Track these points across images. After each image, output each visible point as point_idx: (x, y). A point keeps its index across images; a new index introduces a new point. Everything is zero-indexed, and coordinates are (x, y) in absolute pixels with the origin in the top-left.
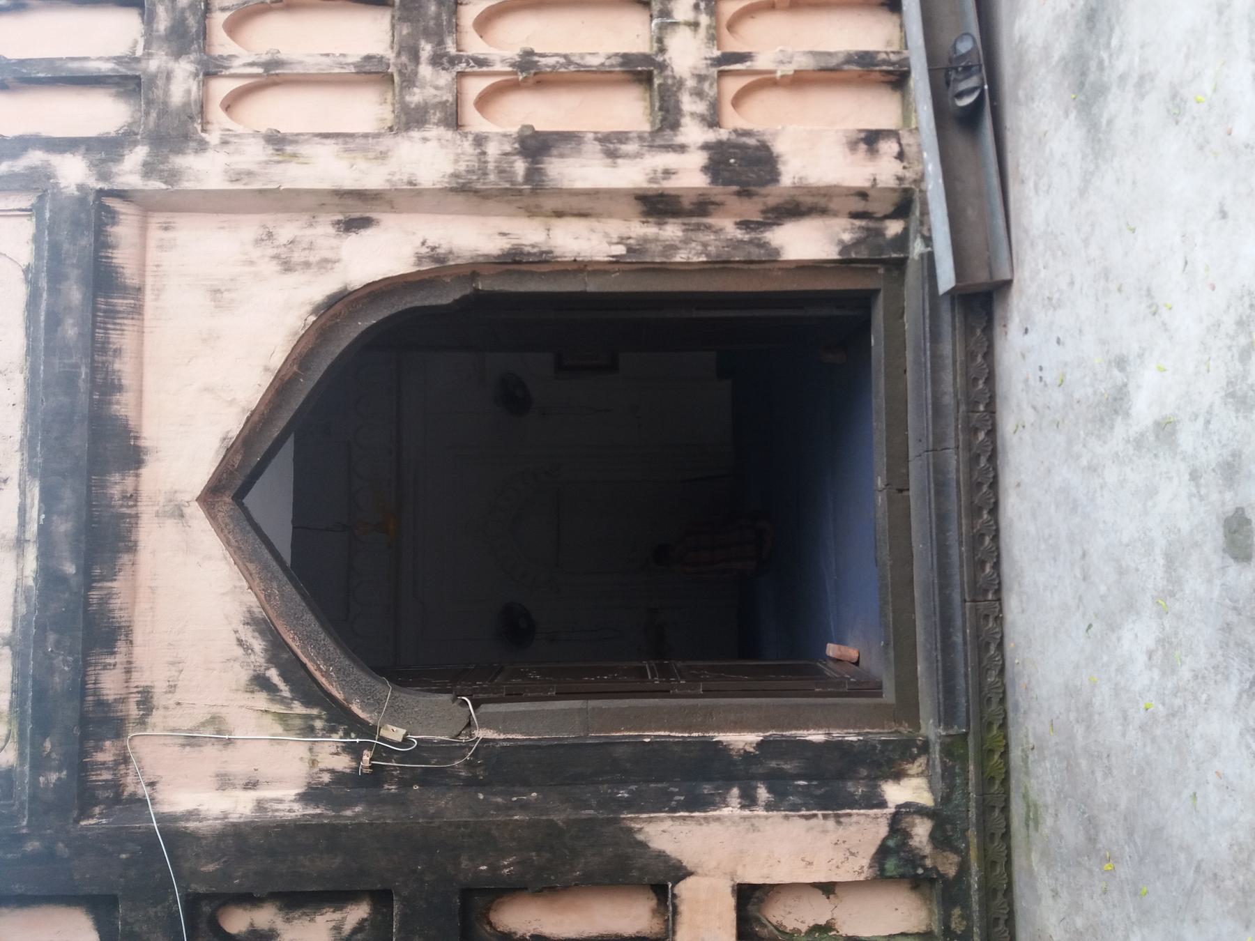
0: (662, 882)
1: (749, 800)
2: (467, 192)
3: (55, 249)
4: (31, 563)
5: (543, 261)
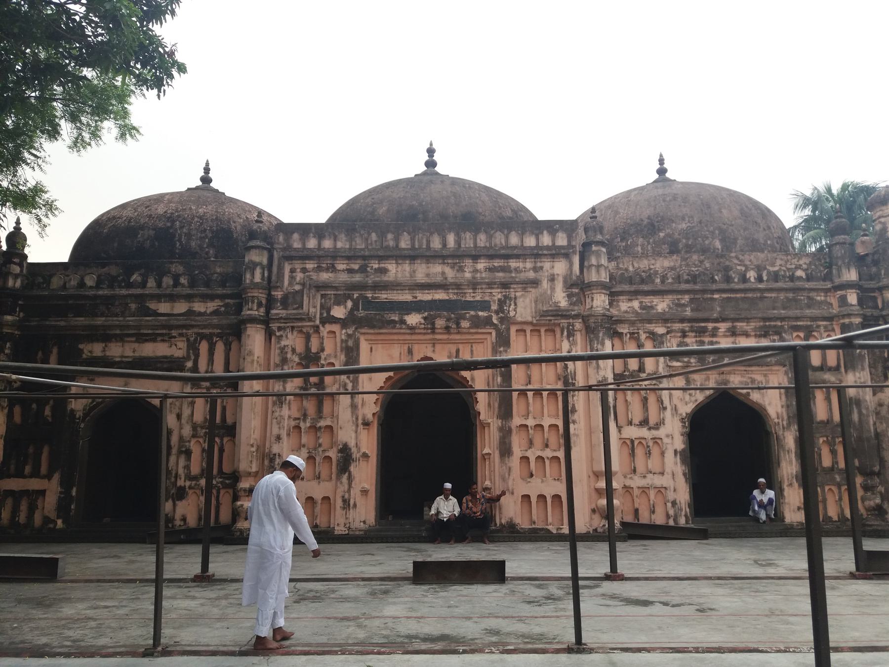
0: (49, 477)
1: (61, 493)
2: (181, 438)
3: (174, 362)
4: (117, 359)
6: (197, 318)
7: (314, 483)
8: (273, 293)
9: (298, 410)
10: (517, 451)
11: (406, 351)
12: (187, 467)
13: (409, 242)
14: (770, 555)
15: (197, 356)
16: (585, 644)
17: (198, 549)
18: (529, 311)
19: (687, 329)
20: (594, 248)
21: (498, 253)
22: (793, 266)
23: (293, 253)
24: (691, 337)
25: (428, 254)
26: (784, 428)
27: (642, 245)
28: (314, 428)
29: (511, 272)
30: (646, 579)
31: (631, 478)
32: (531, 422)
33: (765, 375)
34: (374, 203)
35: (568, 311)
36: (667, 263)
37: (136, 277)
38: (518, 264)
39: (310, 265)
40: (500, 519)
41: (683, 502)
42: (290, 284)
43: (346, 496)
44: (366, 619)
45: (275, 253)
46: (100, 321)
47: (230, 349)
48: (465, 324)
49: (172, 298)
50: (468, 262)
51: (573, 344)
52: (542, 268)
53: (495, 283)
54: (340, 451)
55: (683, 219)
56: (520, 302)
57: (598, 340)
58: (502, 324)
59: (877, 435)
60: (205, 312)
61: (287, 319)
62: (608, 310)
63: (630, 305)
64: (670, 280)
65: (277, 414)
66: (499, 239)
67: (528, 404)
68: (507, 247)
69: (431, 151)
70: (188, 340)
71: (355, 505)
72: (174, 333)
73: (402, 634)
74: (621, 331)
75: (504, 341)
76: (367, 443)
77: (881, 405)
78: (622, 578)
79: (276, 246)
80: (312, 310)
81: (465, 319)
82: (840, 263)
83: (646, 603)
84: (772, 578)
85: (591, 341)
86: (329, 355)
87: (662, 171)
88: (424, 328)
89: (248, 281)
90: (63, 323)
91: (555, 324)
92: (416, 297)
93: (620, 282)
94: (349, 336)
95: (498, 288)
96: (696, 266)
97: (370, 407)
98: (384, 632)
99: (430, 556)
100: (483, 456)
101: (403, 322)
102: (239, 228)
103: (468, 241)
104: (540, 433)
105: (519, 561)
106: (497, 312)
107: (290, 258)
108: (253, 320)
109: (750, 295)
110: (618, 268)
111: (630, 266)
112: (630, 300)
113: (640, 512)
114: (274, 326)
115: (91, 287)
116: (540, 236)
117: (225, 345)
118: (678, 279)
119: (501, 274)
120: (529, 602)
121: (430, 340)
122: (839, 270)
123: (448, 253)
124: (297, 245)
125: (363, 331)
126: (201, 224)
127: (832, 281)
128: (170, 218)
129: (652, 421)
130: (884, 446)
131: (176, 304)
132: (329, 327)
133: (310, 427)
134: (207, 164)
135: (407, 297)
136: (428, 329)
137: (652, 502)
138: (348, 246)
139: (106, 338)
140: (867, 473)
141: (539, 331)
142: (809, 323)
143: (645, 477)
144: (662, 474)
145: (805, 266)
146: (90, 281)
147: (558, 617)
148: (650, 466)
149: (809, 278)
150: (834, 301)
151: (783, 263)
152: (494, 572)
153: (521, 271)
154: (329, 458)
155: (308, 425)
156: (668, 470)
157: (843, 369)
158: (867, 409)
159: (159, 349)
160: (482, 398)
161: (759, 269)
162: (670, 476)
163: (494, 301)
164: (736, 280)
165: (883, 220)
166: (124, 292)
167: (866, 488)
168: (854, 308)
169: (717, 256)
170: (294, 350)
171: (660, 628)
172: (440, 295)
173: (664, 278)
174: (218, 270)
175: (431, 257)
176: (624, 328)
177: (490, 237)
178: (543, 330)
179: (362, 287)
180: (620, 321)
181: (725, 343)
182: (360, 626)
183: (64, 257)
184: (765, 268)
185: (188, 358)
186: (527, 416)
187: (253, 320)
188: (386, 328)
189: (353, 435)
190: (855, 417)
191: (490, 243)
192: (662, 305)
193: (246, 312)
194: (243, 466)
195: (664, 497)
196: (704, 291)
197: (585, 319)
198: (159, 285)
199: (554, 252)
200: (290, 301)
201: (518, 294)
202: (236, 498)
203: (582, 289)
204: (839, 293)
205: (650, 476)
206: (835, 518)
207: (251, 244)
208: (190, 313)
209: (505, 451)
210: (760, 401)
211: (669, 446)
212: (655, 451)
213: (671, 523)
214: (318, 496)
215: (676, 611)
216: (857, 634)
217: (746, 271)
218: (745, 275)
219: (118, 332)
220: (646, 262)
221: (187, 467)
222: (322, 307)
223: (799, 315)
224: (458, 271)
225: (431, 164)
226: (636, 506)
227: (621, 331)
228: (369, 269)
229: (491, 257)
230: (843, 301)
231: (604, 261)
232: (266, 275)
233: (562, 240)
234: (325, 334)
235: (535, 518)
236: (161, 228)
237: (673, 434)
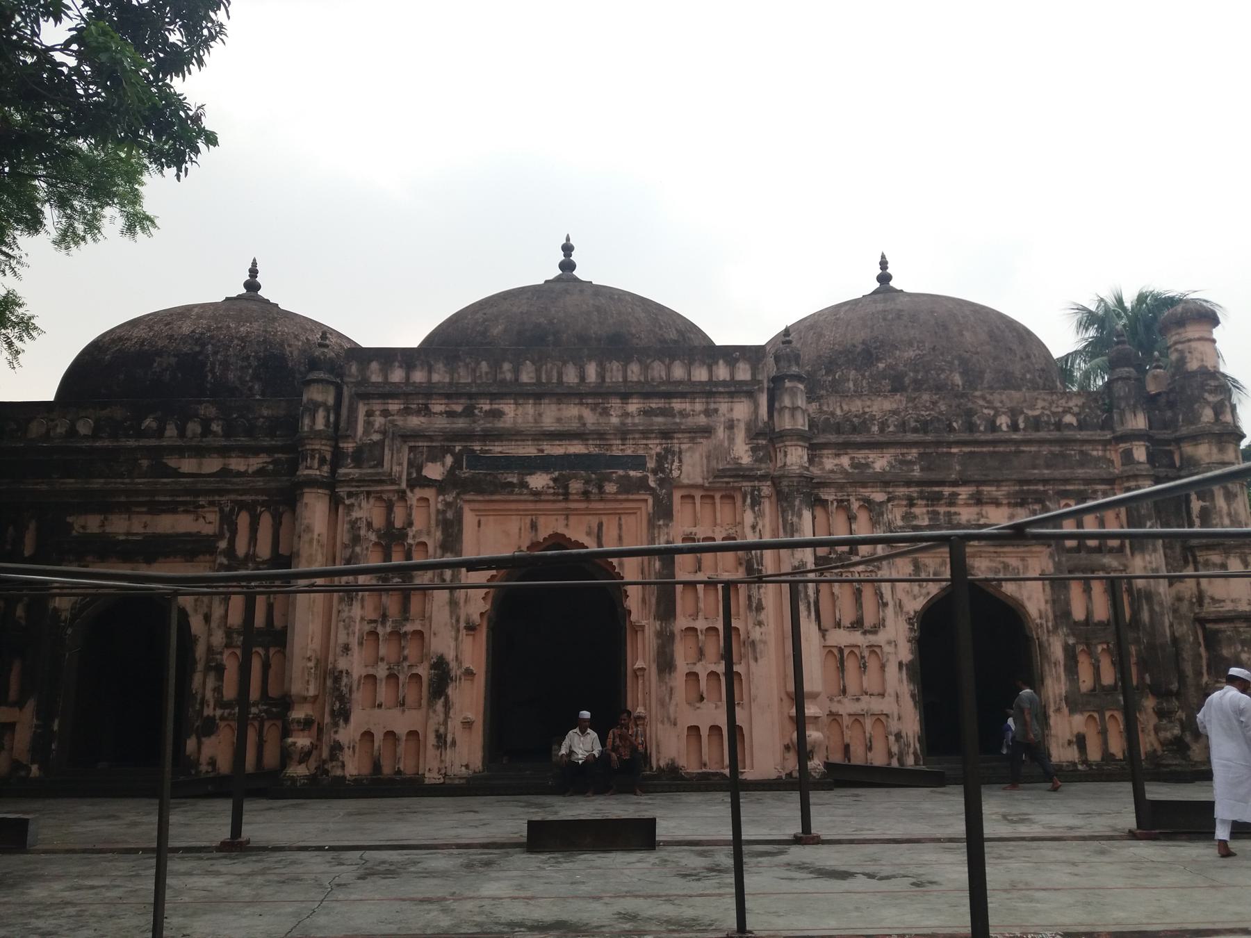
0: (20, 704)
1: (37, 727)
2: (210, 649)
4: (122, 538)
5: (194, 671)
6: (235, 480)
7: (396, 712)
8: (341, 445)
9: (375, 609)
10: (682, 664)
11: (528, 525)
12: (218, 690)
13: (533, 375)
14: (1025, 808)
15: (234, 532)
16: (750, 932)
17: (226, 805)
18: (698, 469)
19: (915, 495)
20: (788, 384)
21: (657, 389)
22: (1060, 410)
23: (371, 390)
24: (921, 506)
25: (559, 391)
26: (1048, 632)
27: (855, 381)
28: (397, 635)
29: (674, 416)
30: (851, 842)
31: (839, 702)
32: (701, 624)
33: (1023, 559)
34: (485, 320)
35: (752, 469)
36: (888, 405)
37: (149, 422)
38: (683, 406)
39: (394, 406)
40: (658, 760)
41: (911, 734)
42: (366, 432)
43: (442, 730)
44: (455, 900)
45: (345, 388)
46: (97, 483)
47: (281, 523)
48: (610, 488)
49: (200, 452)
50: (615, 403)
51: (759, 515)
52: (716, 411)
53: (652, 432)
54: (434, 666)
55: (911, 344)
56: (686, 458)
57: (792, 507)
58: (661, 488)
59: (1175, 640)
60: (246, 471)
61: (361, 481)
62: (807, 469)
63: (836, 461)
64: (891, 429)
65: (344, 615)
66: (658, 370)
67: (697, 599)
68: (669, 382)
69: (568, 249)
70: (221, 511)
71: (454, 743)
72: (202, 500)
73: (503, 921)
74: (826, 497)
75: (664, 512)
76: (472, 655)
77: (1179, 599)
78: (817, 841)
79: (347, 379)
80: (396, 468)
81: (610, 481)
82: (1123, 405)
83: (844, 875)
84: (1023, 839)
85: (784, 511)
86: (420, 532)
87: (884, 278)
88: (554, 494)
89: (306, 429)
90: (44, 487)
91: (734, 488)
92: (542, 451)
93: (824, 431)
94: (448, 505)
95: (656, 438)
96: (927, 409)
97: (476, 605)
98: (477, 919)
99: (556, 813)
100: (635, 671)
101: (524, 485)
102: (296, 353)
103: (615, 373)
104: (714, 638)
105: (680, 819)
106: (655, 472)
107: (365, 397)
108: (313, 483)
109: (1001, 449)
110: (821, 411)
111: (837, 408)
112: (838, 455)
113: (852, 748)
114: (342, 491)
115: (85, 436)
116: (714, 368)
117: (274, 517)
118: (903, 426)
119: (660, 419)
120: (685, 876)
121: (562, 510)
122: (1122, 414)
123: (588, 390)
124: (376, 378)
125: (467, 497)
126: (243, 348)
127: (1112, 429)
128: (199, 340)
129: (869, 621)
130: (1185, 655)
131: (204, 461)
132: (419, 493)
133: (391, 633)
134: (254, 264)
135: (529, 450)
136: (558, 494)
137: (868, 735)
138: (447, 380)
139: (105, 505)
140: (1160, 692)
141: (713, 497)
142: (1082, 487)
143: (858, 700)
144: (882, 695)
145: (1076, 410)
146: (84, 428)
147: (720, 895)
148: (865, 685)
149: (1082, 426)
150: (1115, 457)
151: (1046, 404)
152: (640, 836)
153: (688, 415)
154: (417, 677)
155: (389, 629)
156: (890, 690)
157: (1128, 551)
158: (1161, 604)
159: (183, 524)
160: (634, 593)
161: (1014, 413)
162: (893, 699)
163: (651, 457)
164: (982, 428)
165: (1179, 347)
166: (132, 443)
167: (1161, 713)
168: (1142, 467)
169: (956, 396)
170: (369, 525)
171: (857, 909)
172: (576, 448)
173: (883, 426)
174: (265, 413)
175: (563, 395)
176: (829, 494)
177: (645, 368)
178: (718, 496)
179: (468, 436)
180: (823, 485)
181: (966, 514)
182: (445, 911)
183: (50, 396)
184: (1022, 412)
185: (219, 536)
186: (695, 616)
187: (313, 483)
188: (500, 494)
189: (452, 644)
190: (1145, 616)
191: (646, 377)
192: (880, 462)
193: (303, 472)
194: (296, 688)
195: (885, 727)
196: (938, 444)
197: (775, 481)
198: (182, 433)
199: (733, 389)
200: (365, 456)
201: (683, 447)
202: (286, 733)
203: (771, 440)
204: (1123, 446)
205: (865, 698)
206: (1120, 756)
207: (312, 376)
208: (225, 472)
209: (666, 664)
210: (1017, 595)
211: (892, 658)
212: (873, 664)
213: (895, 763)
214: (402, 731)
215: (884, 886)
216: (1122, 915)
217: (997, 414)
218: (994, 422)
219: (123, 499)
220: (859, 403)
221: (218, 690)
222: (410, 464)
223: (1068, 476)
224: (601, 414)
225: (567, 266)
226: (847, 740)
227: (824, 497)
228: (476, 411)
229: (646, 396)
230: (1128, 456)
231: (801, 402)
232: (332, 419)
233: (743, 373)
234: (414, 502)
235: (705, 758)
236: (186, 354)
237: (897, 639)
